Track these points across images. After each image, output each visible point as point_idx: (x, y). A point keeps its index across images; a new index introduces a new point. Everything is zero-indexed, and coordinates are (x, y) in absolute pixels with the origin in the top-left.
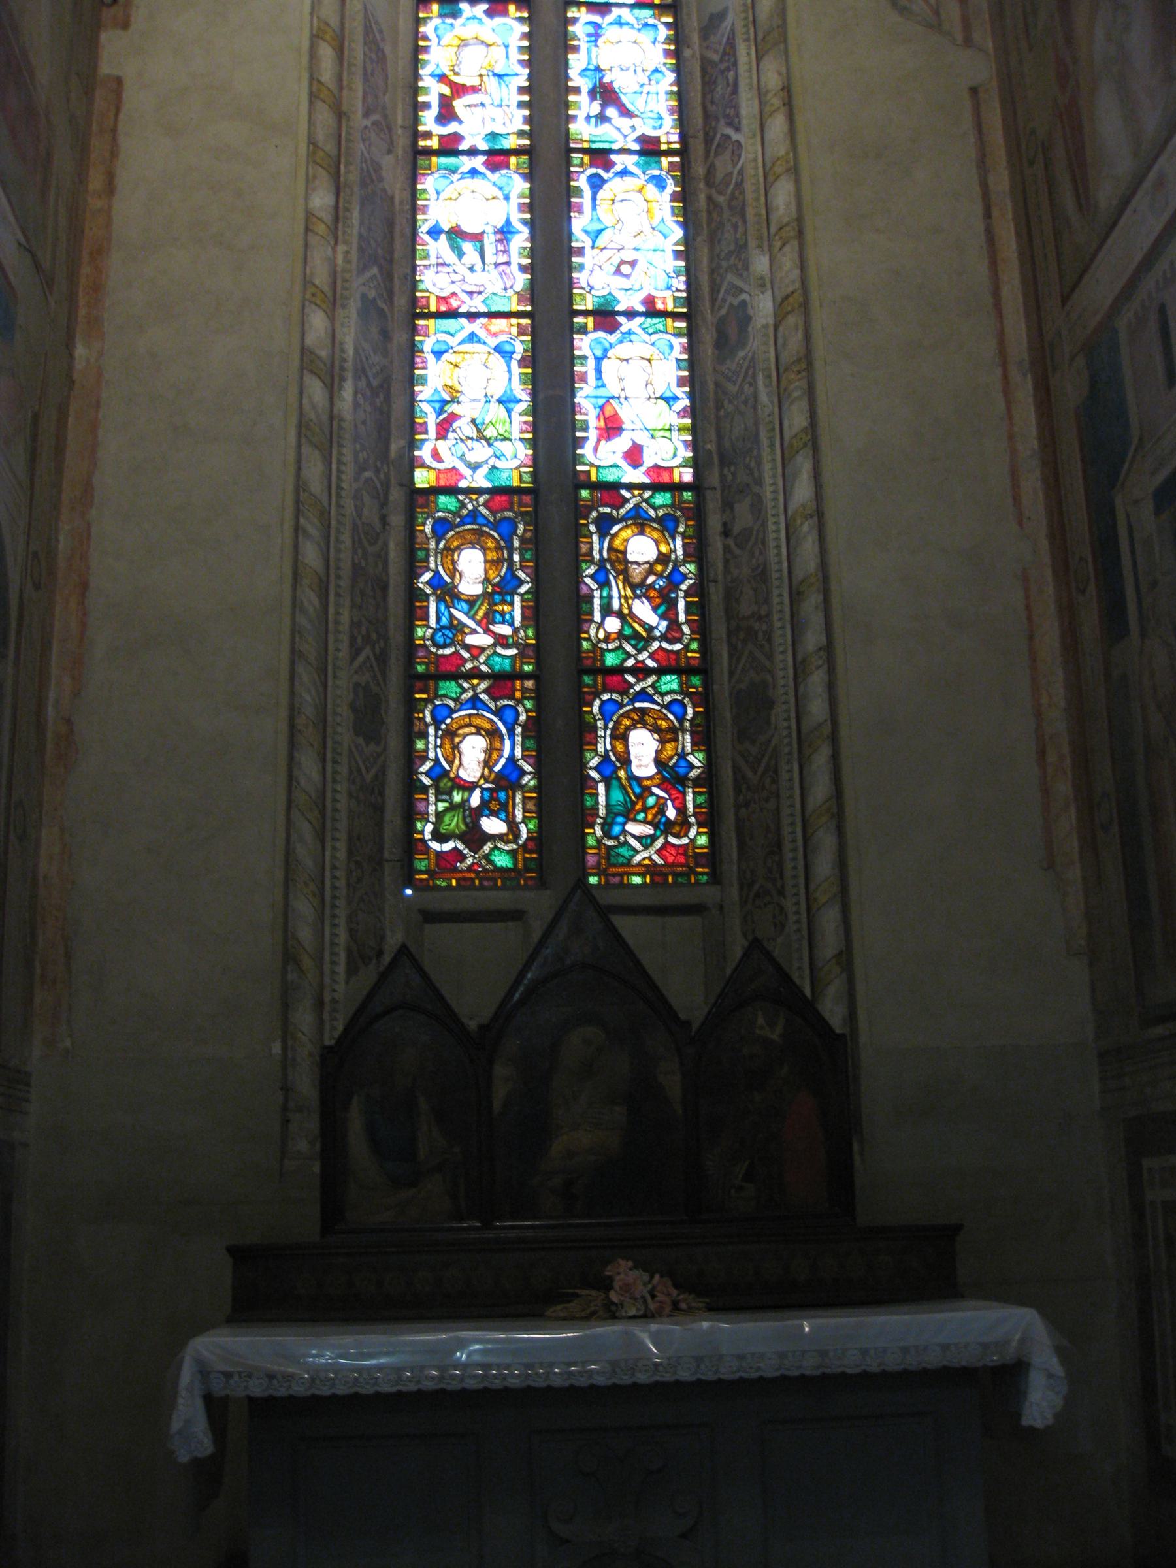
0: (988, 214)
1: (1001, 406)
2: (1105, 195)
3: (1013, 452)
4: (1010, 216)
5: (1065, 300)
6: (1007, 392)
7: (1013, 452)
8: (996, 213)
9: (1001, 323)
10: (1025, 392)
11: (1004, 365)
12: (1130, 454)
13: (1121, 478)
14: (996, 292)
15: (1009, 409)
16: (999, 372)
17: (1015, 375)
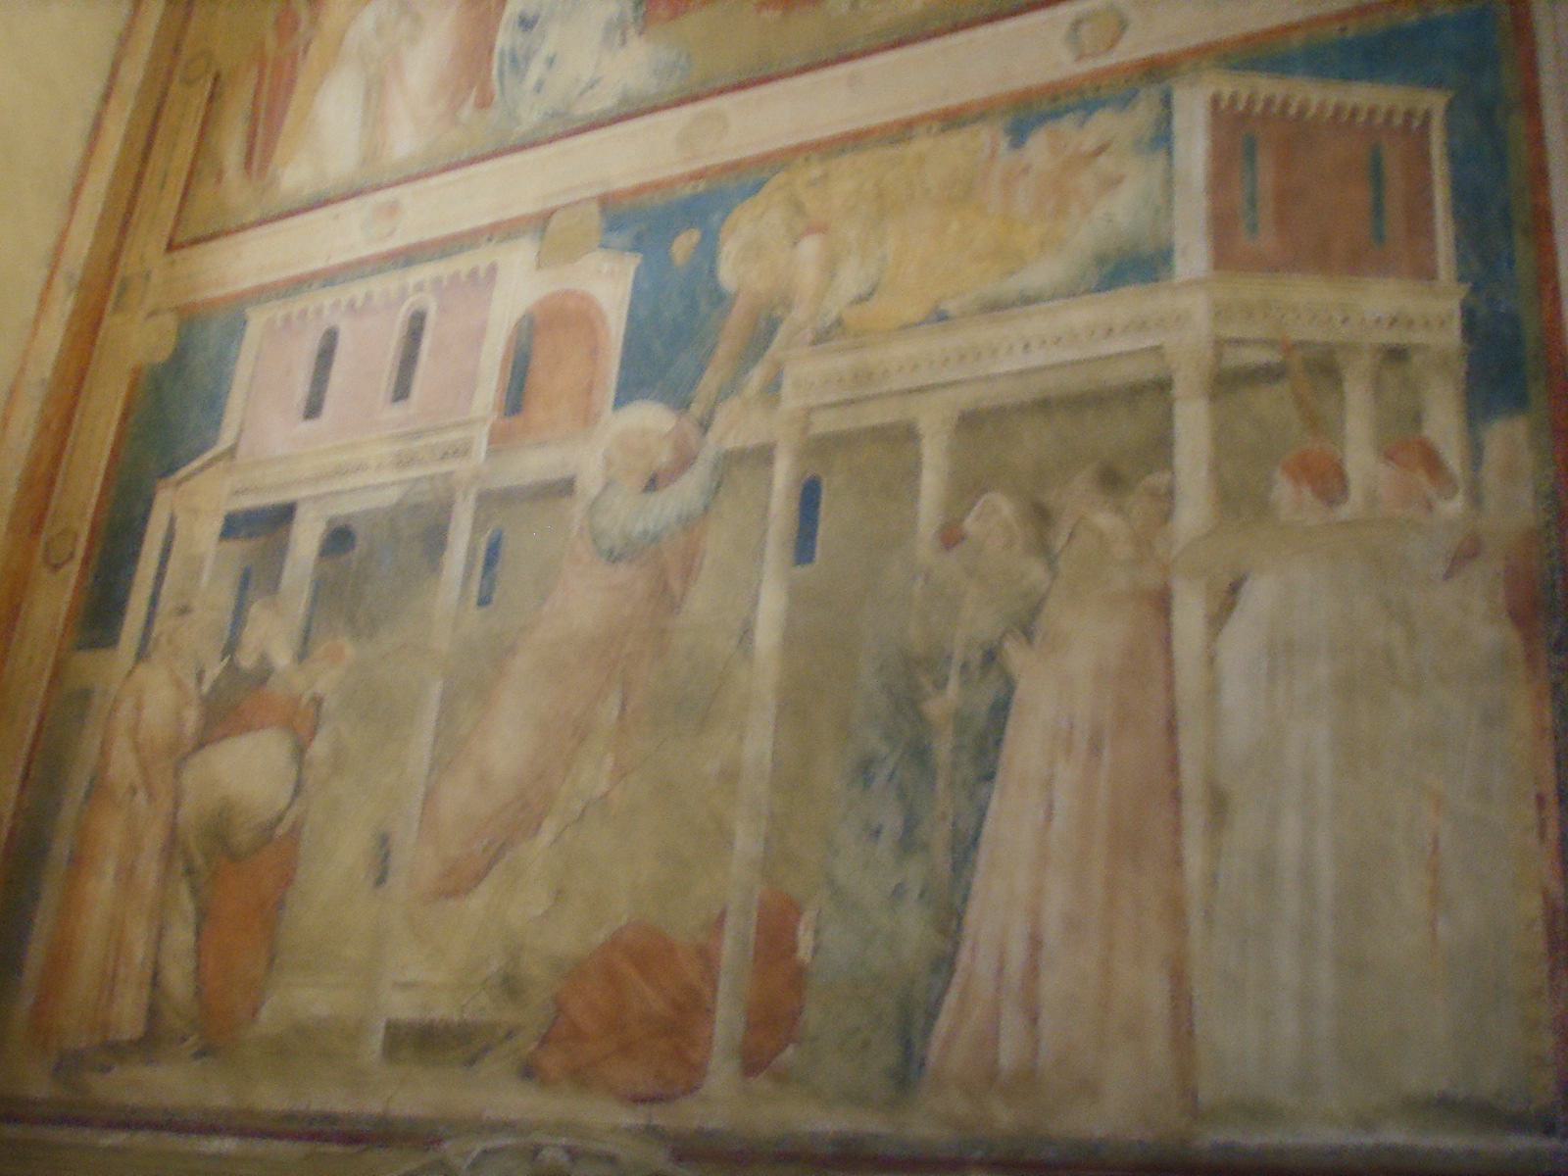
0: (106, 97)
1: (32, 308)
2: (294, 175)
3: (22, 371)
4: (127, 114)
5: (171, 247)
6: (43, 302)
7: (22, 371)
8: (113, 103)
9: (70, 221)
10: (63, 305)
11: (54, 268)
12: (208, 455)
13: (182, 472)
14: (77, 190)
15: (37, 320)
16: (44, 272)
17: (61, 286)
